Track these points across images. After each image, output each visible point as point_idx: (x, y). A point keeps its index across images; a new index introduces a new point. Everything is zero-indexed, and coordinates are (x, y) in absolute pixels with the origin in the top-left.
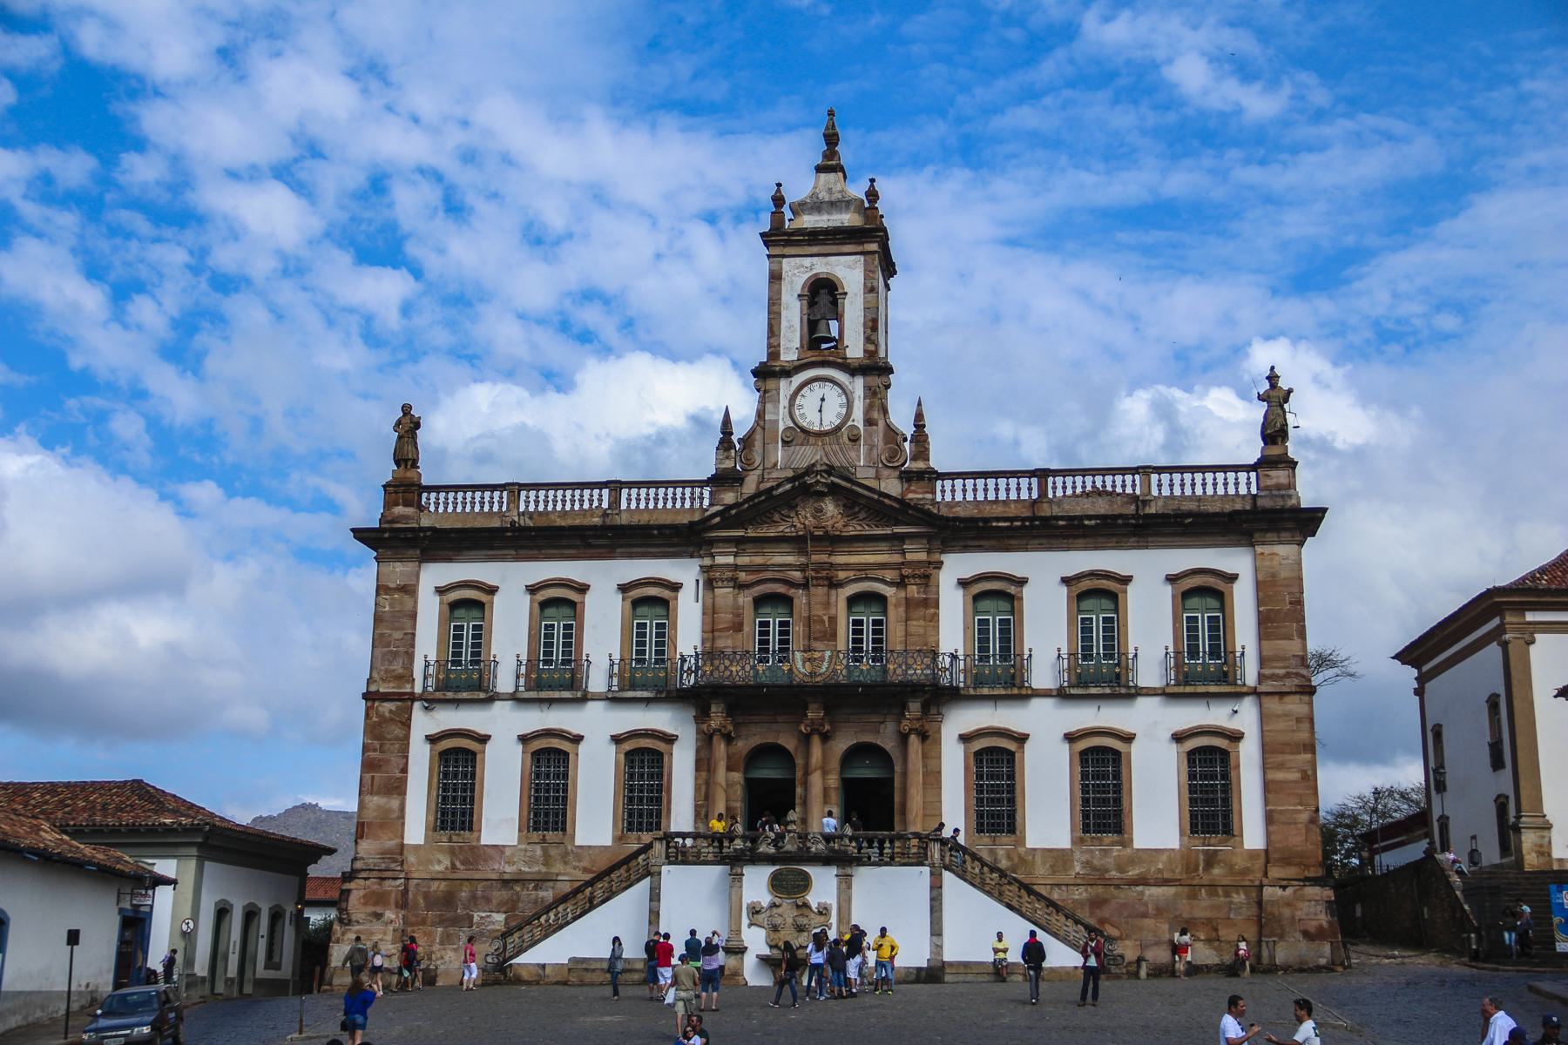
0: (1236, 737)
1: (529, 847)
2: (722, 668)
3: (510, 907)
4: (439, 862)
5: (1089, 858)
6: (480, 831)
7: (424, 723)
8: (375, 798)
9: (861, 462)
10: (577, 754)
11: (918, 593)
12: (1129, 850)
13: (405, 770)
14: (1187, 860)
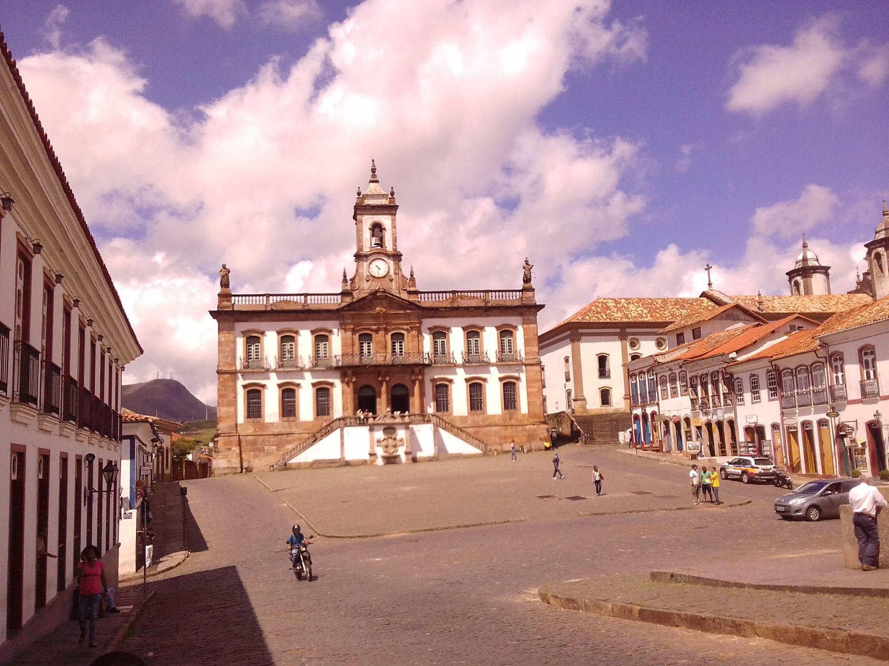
0: (518, 379)
3: (279, 445)
4: (250, 429)
6: (264, 417)
7: (241, 382)
9: (394, 288)
12: (485, 416)
14: (503, 417)
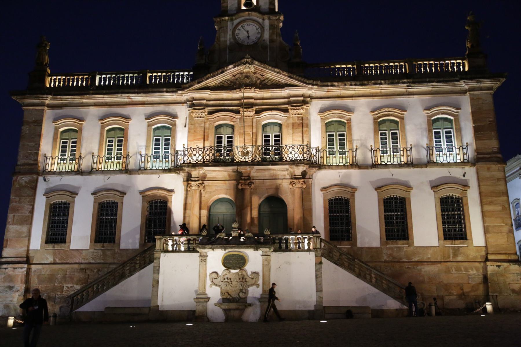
1: (95, 251)
2: (197, 155)
5: (391, 252)
6: (70, 242)
8: (15, 226)
10: (122, 203)
11: (298, 120)
12: (412, 248)
13: (32, 212)
